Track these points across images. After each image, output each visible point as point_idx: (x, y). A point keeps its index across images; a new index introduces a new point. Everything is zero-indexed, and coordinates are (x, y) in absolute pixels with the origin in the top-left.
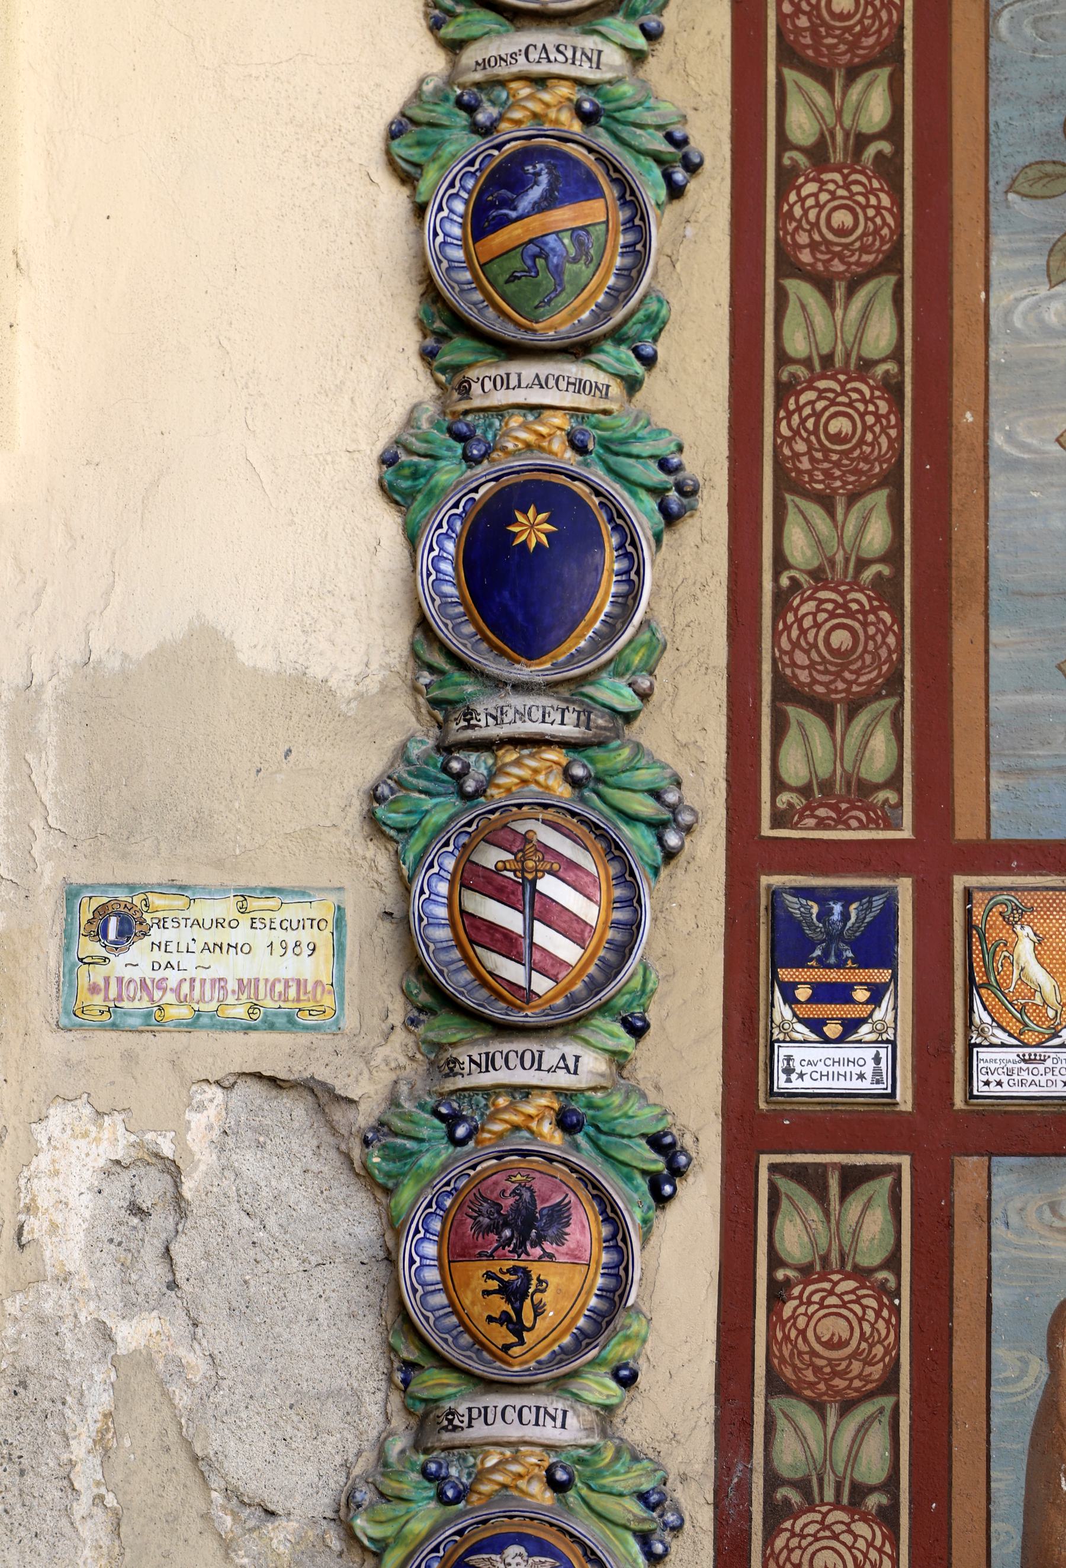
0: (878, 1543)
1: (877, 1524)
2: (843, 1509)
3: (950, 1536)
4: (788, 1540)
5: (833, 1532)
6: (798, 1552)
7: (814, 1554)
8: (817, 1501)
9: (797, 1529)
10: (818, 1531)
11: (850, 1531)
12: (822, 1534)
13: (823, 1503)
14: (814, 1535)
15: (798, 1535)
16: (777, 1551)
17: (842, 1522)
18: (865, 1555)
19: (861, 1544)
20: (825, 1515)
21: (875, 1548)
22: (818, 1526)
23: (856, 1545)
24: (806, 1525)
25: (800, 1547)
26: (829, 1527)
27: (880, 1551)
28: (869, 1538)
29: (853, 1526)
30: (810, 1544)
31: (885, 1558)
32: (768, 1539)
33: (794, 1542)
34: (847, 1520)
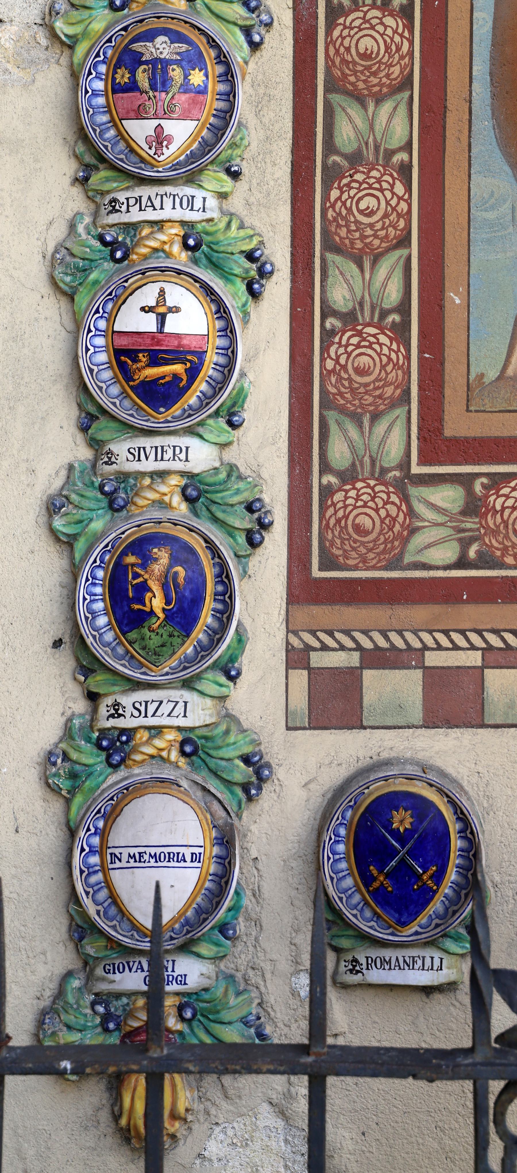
0: (400, 30)
1: (399, 17)
2: (378, 8)
3: (447, 23)
4: (342, 31)
5: (371, 24)
6: (348, 39)
7: (358, 40)
8: (361, 4)
9: (348, 24)
10: (361, 24)
11: (382, 23)
12: (363, 26)
13: (364, 5)
14: (359, 27)
15: (348, 28)
16: (334, 39)
17: (377, 18)
18: (392, 39)
19: (389, 32)
20: (366, 13)
21: (398, 34)
22: (361, 21)
23: (386, 33)
24: (353, 20)
25: (349, 35)
26: (368, 21)
27: (401, 36)
28: (395, 27)
29: (384, 20)
30: (356, 33)
31: (404, 40)
32: (329, 32)
33: (346, 32)
34: (380, 16)
